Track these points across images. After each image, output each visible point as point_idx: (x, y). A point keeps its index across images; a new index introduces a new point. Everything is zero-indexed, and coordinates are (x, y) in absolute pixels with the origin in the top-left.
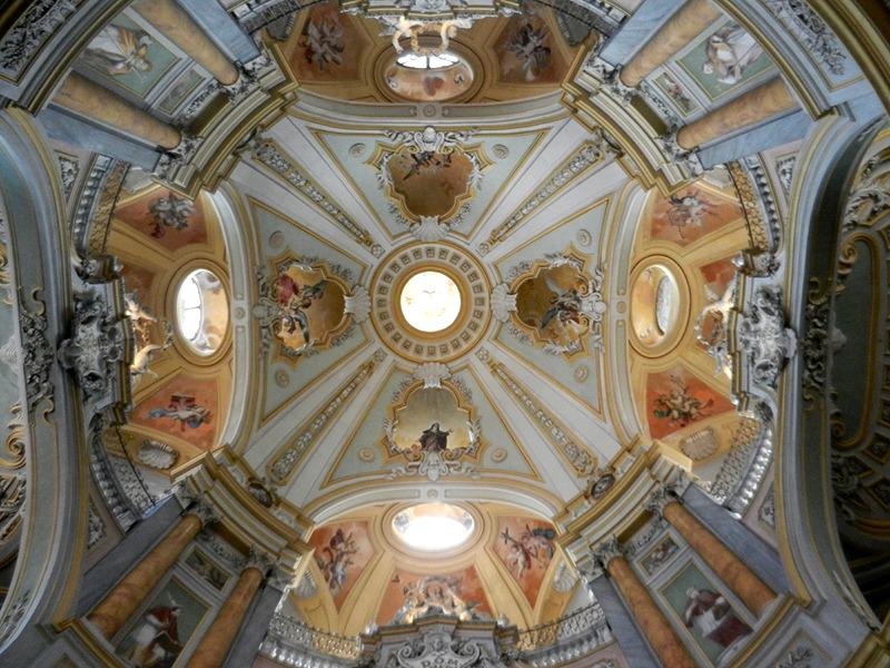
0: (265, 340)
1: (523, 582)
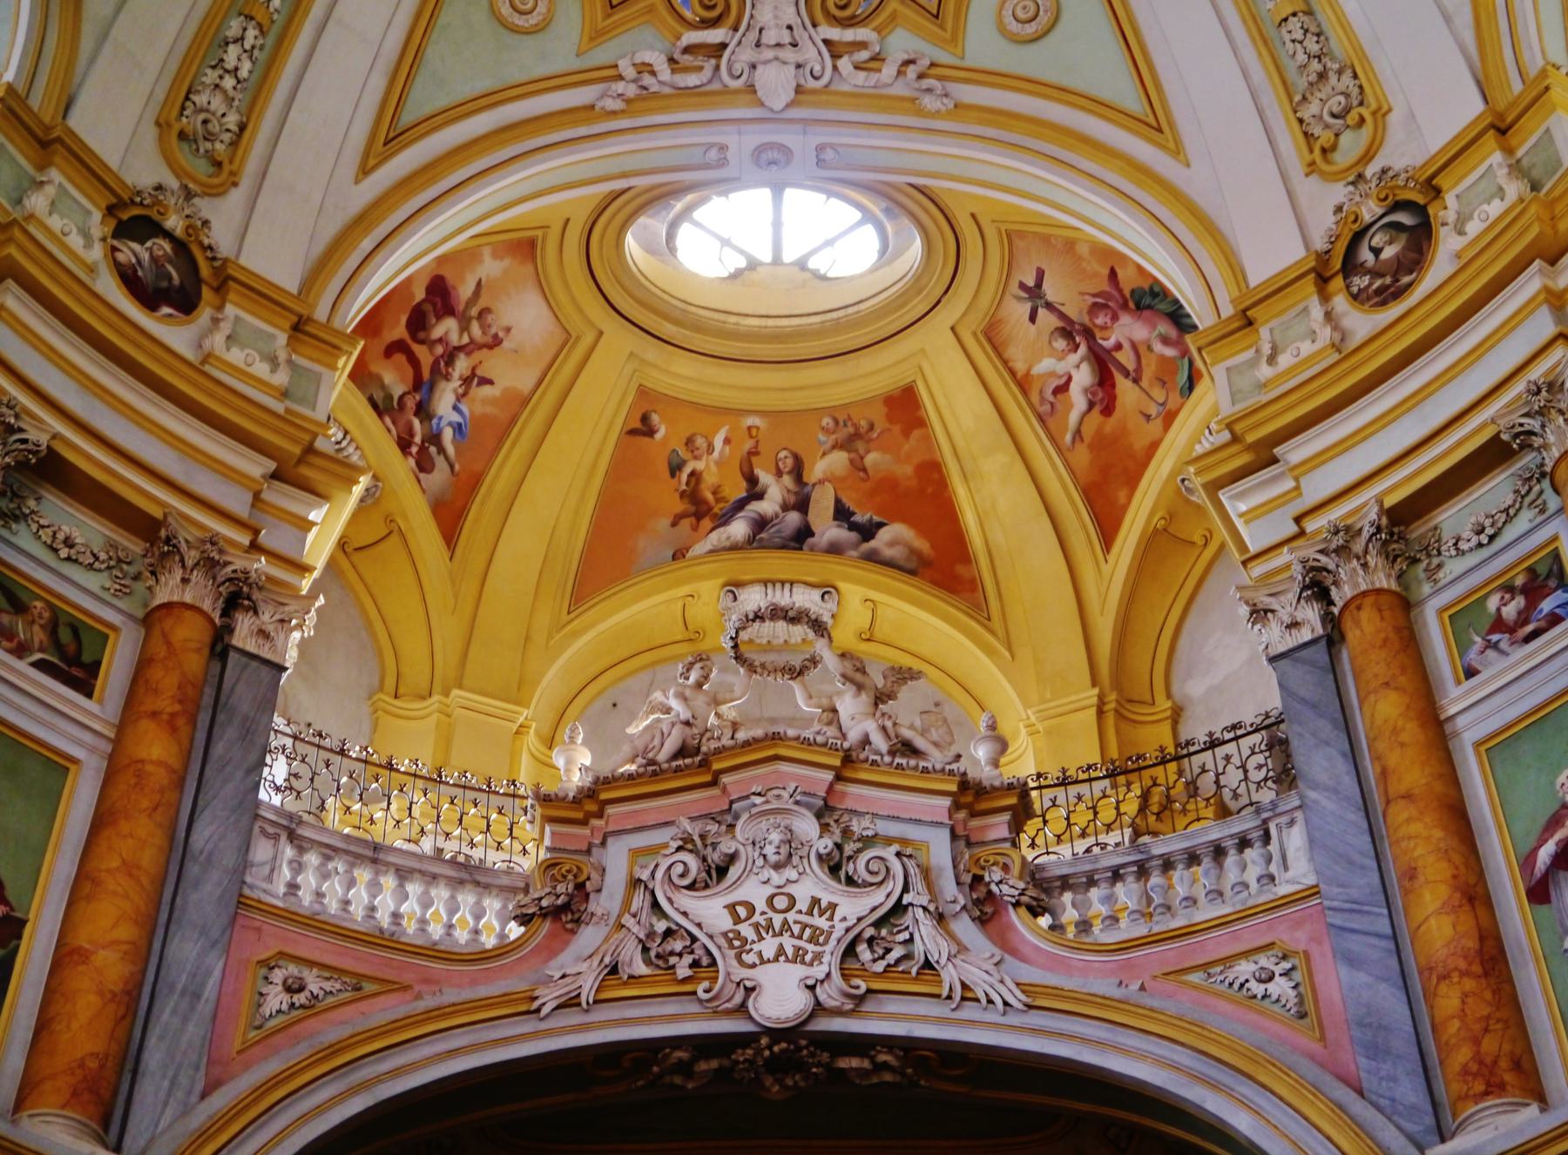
1: (1082, 456)
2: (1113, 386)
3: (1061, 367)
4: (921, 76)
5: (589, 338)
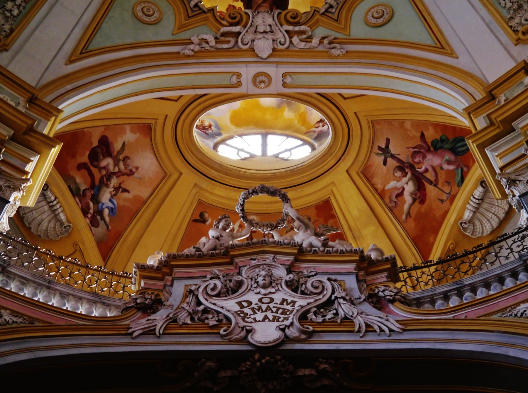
1: (411, 224)
2: (425, 190)
3: (399, 185)
4: (330, 43)
5: (175, 176)
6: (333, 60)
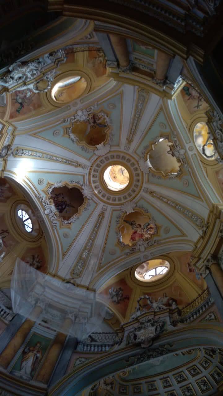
0: (153, 244)
6: (178, 132)
